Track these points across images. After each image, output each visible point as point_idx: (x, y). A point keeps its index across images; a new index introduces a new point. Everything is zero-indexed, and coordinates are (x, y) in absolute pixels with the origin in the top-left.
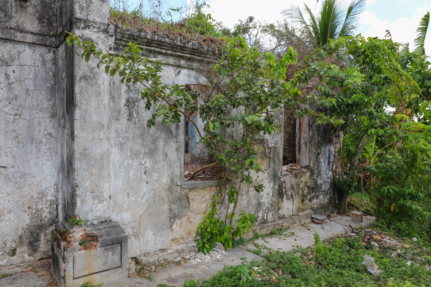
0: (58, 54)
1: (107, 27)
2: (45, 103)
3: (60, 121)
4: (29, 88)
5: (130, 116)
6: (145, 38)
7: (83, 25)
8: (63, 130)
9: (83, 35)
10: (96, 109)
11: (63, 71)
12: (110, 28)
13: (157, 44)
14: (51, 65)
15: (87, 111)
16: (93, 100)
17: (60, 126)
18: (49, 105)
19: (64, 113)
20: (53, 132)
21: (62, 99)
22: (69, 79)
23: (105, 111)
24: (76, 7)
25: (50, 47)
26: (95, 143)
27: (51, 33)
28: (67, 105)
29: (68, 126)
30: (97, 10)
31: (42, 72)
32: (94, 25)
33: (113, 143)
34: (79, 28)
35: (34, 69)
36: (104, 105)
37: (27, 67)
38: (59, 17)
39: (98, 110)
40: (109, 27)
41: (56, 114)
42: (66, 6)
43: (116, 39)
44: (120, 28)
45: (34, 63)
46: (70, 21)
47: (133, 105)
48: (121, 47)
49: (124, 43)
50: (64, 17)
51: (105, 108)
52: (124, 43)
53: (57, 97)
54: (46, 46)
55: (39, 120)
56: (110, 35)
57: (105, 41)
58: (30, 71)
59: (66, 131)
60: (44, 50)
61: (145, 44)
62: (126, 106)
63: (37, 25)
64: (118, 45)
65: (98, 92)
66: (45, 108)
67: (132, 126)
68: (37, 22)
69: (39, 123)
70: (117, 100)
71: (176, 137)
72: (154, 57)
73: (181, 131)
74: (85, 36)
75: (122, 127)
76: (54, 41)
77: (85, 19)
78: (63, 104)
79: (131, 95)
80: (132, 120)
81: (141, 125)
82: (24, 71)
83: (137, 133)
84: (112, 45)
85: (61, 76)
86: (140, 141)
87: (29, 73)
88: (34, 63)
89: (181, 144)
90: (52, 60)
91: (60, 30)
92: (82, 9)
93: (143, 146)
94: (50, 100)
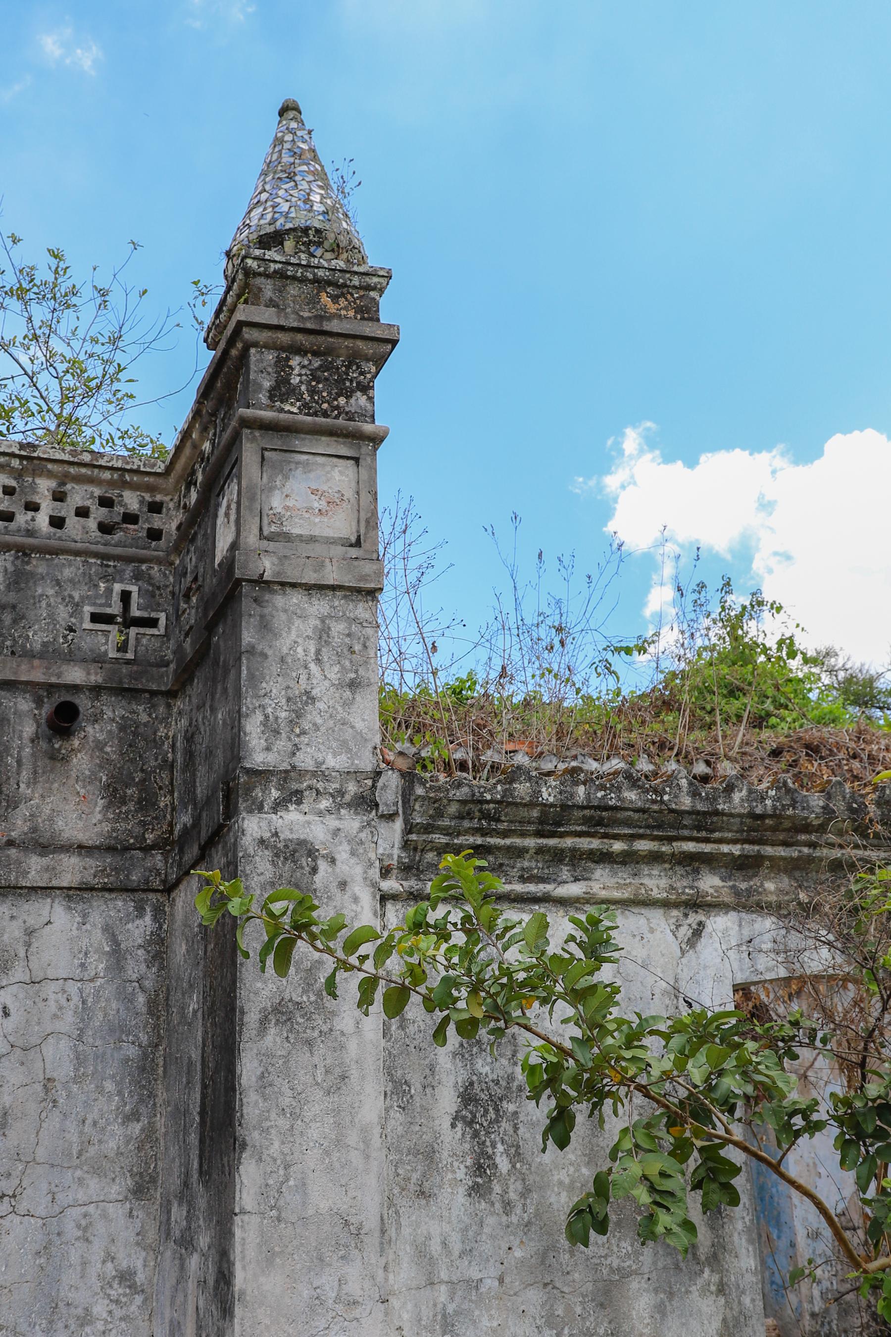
0: (172, 915)
1: (369, 782)
2: (113, 1134)
3: (169, 1212)
4: (55, 1075)
5: (479, 1169)
6: (531, 805)
7: (275, 793)
8: (181, 1259)
9: (276, 834)
10: (327, 1153)
11: (191, 986)
12: (385, 787)
13: (586, 821)
14: (143, 967)
15: (287, 1167)
16: (317, 1109)
17: (168, 1234)
18: (128, 1142)
19: (187, 1174)
20: (139, 1264)
21: (179, 1113)
22: (214, 1024)
23: (367, 1157)
24: (253, 727)
25: (144, 891)
26: (322, 1324)
27: (150, 837)
28: (202, 1141)
29: (204, 1240)
30: (331, 723)
31: (108, 1000)
32: (320, 786)
33: (406, 1316)
34: (260, 809)
35: (81, 991)
36: (365, 1130)
37: (53, 987)
38: (184, 771)
39: (336, 1155)
40: (380, 784)
41: (153, 1180)
42: (213, 729)
43: (409, 829)
44: (423, 783)
45: (82, 965)
46: (227, 784)
47: (492, 1115)
48: (430, 856)
49: (444, 840)
50: (202, 770)
51: (366, 1142)
52: (444, 840)
53: (159, 1101)
54: (127, 890)
55: (85, 1215)
56: (382, 816)
57: (362, 843)
58: (63, 1002)
59: (194, 1262)
60: (121, 904)
61: (532, 828)
62: (460, 1125)
63: (99, 817)
64: (415, 849)
65: (337, 1071)
66: (112, 1155)
67: (491, 1221)
68: (101, 802)
69: (85, 1230)
70: (417, 1099)
71: (715, 1260)
72: (576, 880)
73: (740, 1226)
74: (285, 835)
75: (447, 1228)
76: (160, 865)
77: (285, 766)
78: (186, 1133)
79: (483, 1066)
80: (490, 1190)
81: (537, 1214)
82: (41, 1004)
83: (518, 1253)
84: (390, 856)
85: (183, 1009)
86: (534, 1297)
87: (61, 1008)
88: (82, 965)
89: (747, 1300)
90: (149, 943)
91: (185, 819)
92: (271, 729)
93: (550, 1325)
94: (134, 1116)
